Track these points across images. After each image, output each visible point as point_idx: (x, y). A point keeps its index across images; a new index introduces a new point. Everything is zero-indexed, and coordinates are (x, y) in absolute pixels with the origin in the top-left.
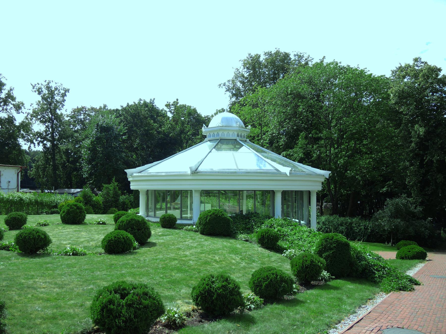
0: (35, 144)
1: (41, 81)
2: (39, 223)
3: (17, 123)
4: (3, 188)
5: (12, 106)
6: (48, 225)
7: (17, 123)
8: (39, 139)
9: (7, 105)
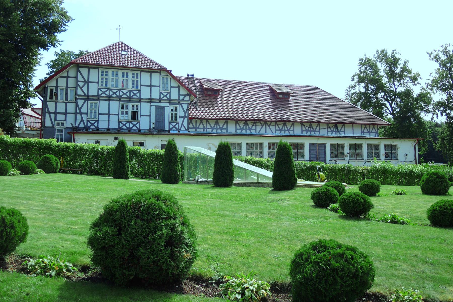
0: (437, 114)
1: (436, 47)
2: (395, 192)
3: (415, 95)
4: (400, 160)
5: (408, 79)
6: (404, 194)
7: (415, 95)
8: (442, 109)
9: (404, 79)
